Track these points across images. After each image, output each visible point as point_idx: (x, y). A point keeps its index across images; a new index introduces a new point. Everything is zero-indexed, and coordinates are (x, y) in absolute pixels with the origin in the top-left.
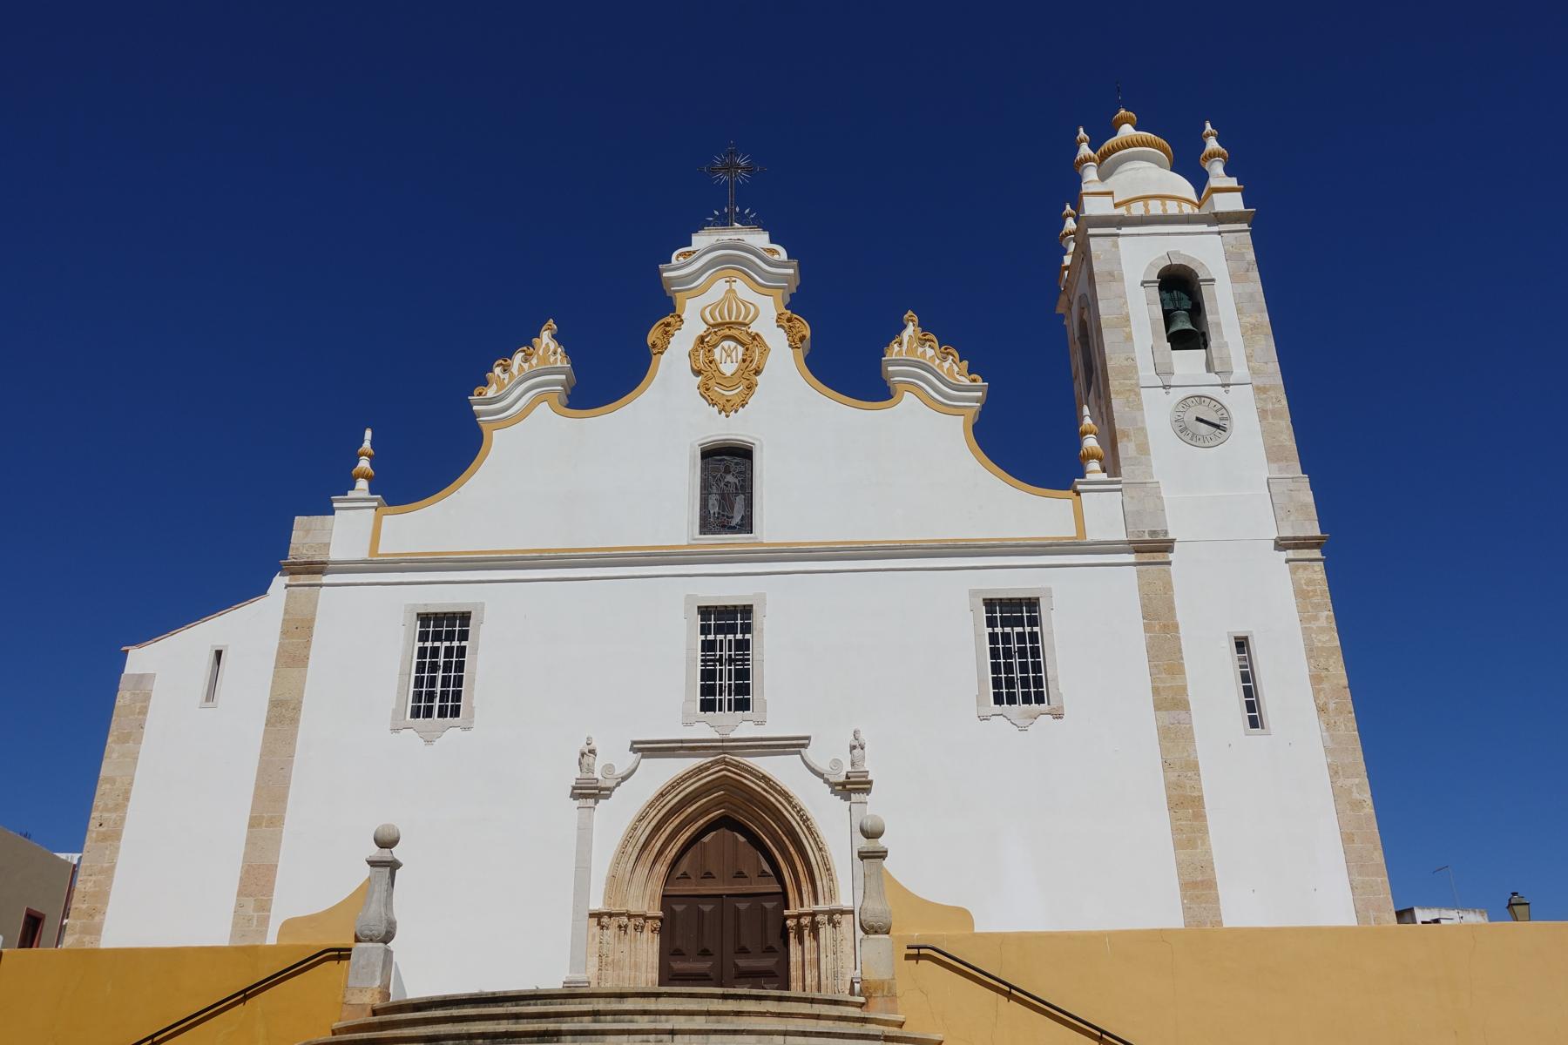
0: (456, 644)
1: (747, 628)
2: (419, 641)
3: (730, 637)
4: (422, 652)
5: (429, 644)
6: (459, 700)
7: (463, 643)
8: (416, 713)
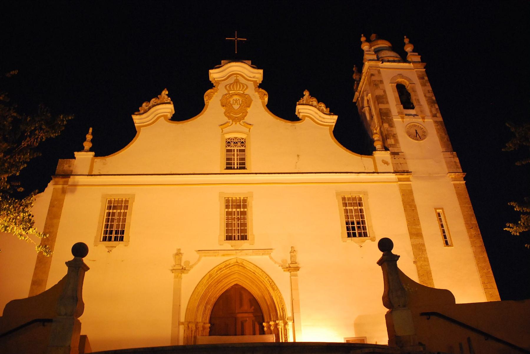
0: (122, 211)
1: (245, 206)
2: (107, 209)
3: (238, 210)
4: (109, 214)
5: (111, 211)
6: (123, 234)
7: (126, 211)
8: (105, 239)
